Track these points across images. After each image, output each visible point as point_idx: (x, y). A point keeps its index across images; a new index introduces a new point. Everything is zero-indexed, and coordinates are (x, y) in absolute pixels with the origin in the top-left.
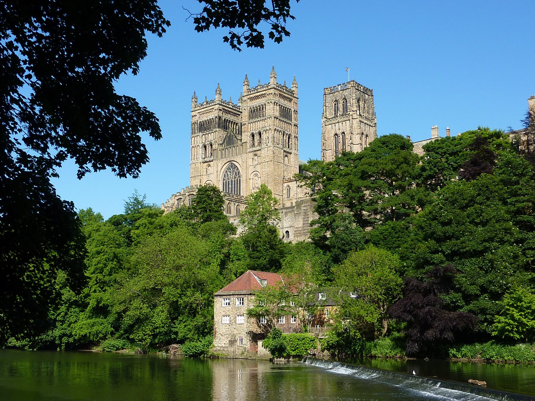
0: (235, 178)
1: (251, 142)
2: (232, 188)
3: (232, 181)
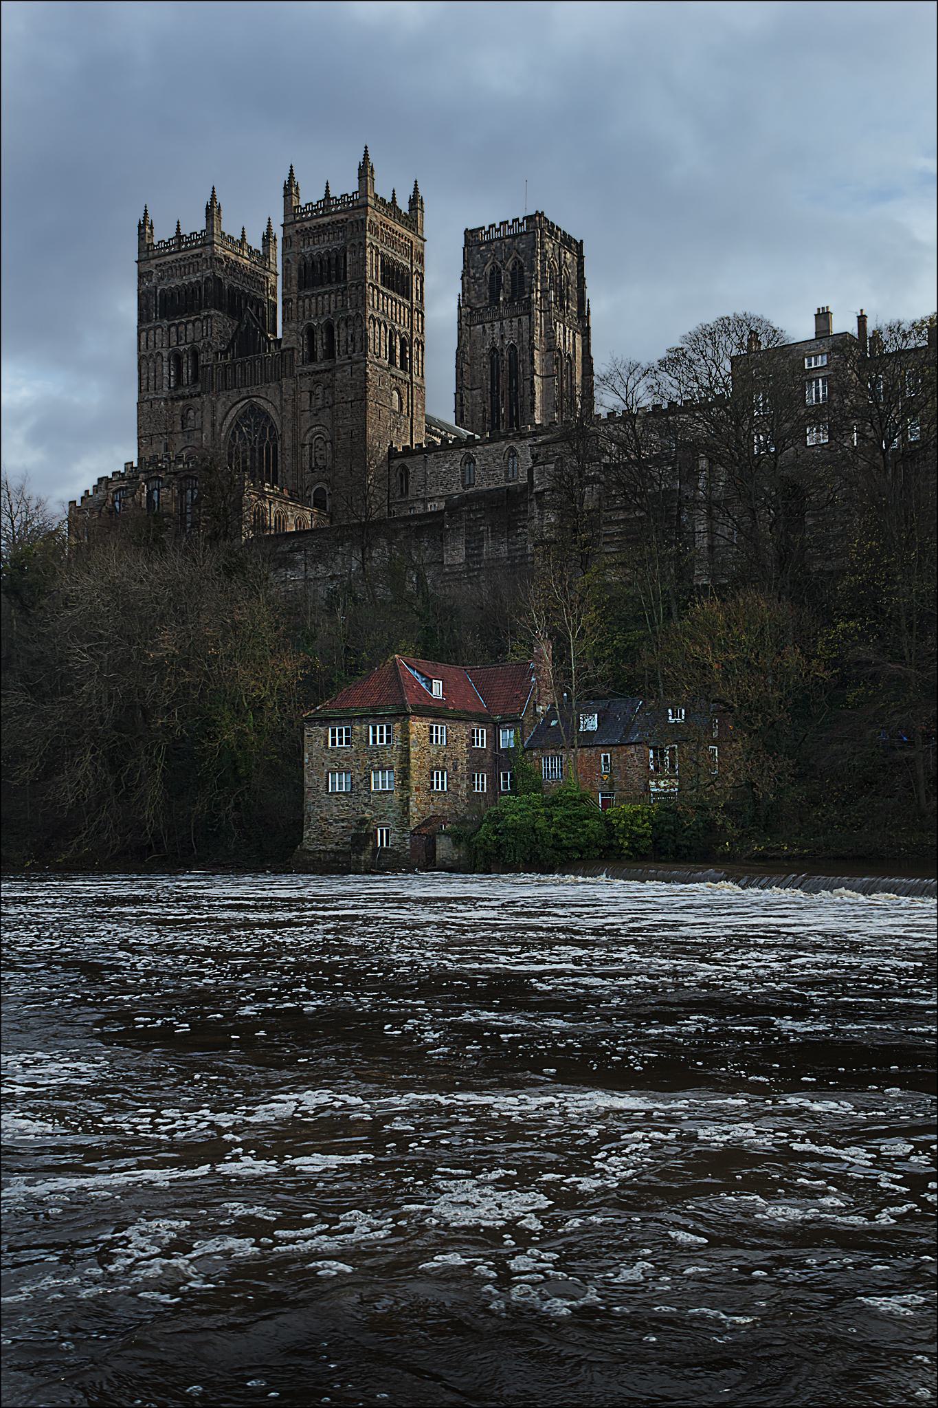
0: (262, 441)
3: (253, 450)
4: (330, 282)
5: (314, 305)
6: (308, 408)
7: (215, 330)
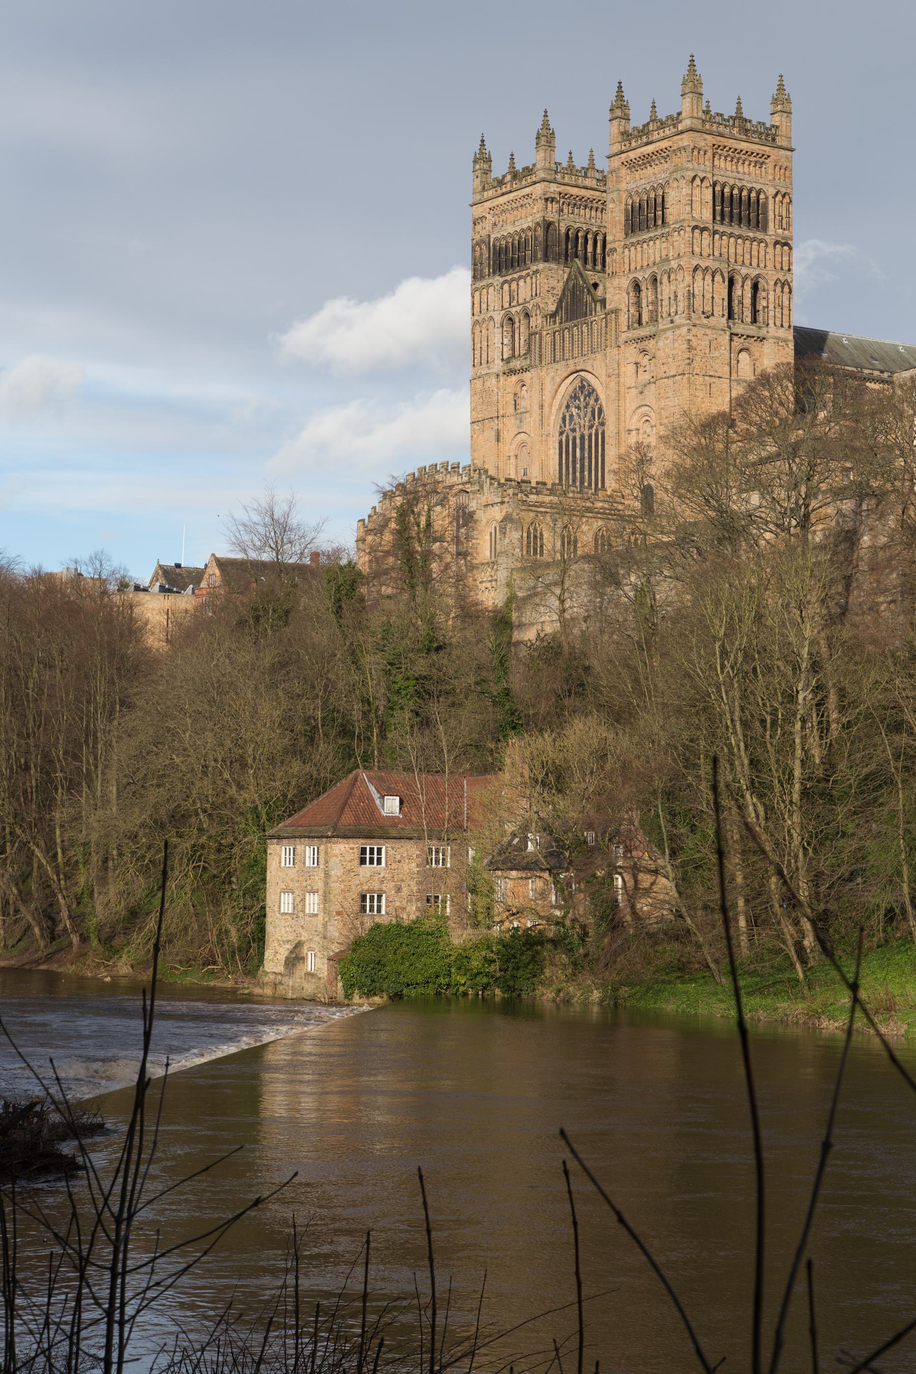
0: (591, 427)
1: (632, 310)
2: (582, 459)
3: (582, 437)
6: (633, 385)
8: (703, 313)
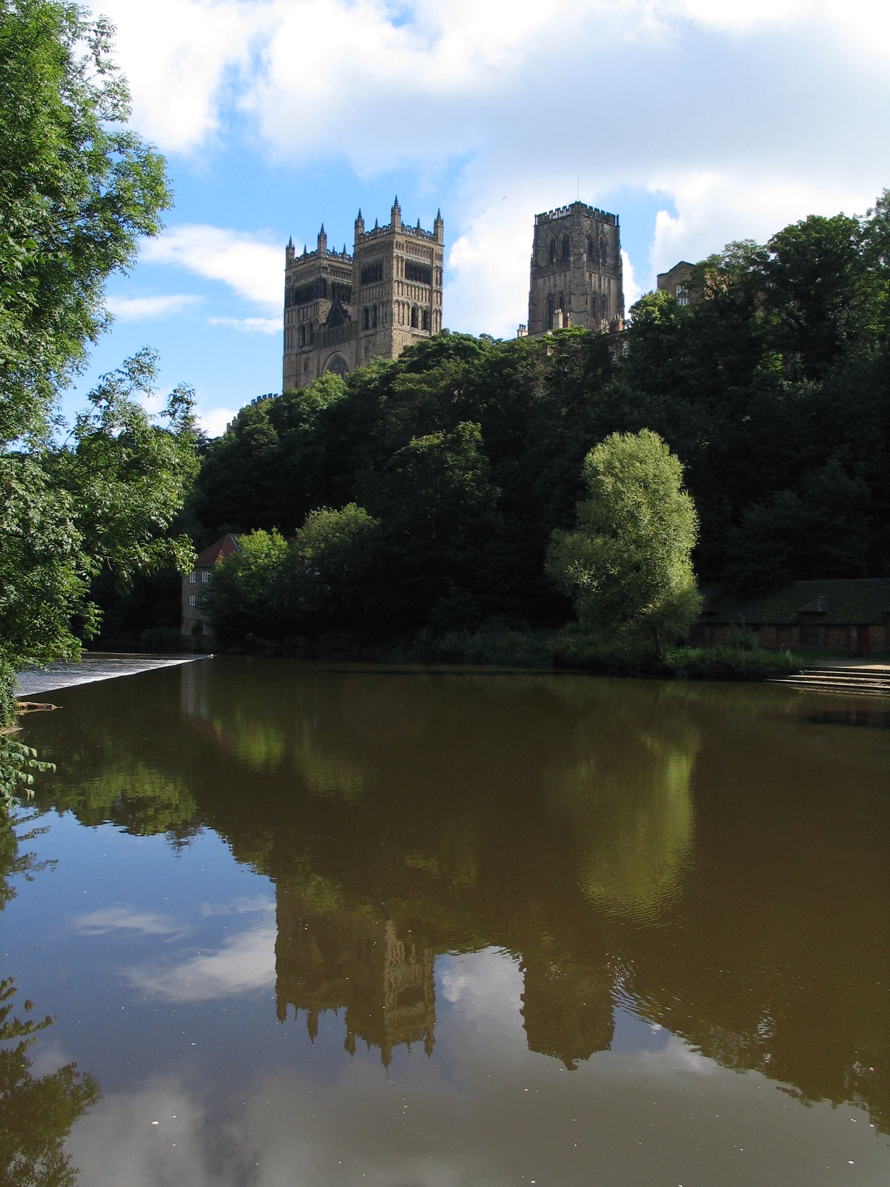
4: (377, 280)
5: (368, 294)
7: (321, 311)
8: (399, 323)
